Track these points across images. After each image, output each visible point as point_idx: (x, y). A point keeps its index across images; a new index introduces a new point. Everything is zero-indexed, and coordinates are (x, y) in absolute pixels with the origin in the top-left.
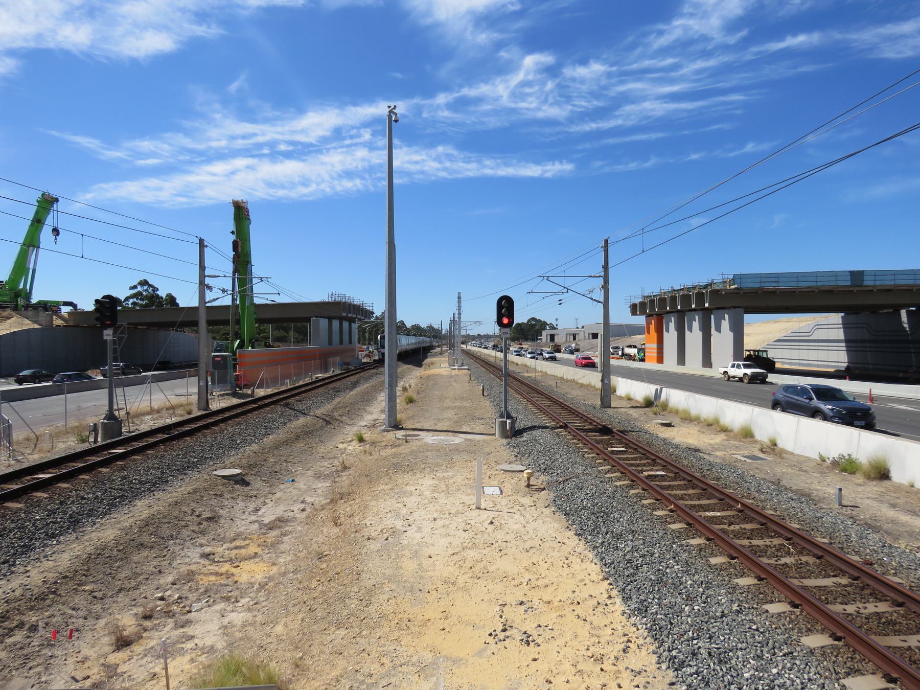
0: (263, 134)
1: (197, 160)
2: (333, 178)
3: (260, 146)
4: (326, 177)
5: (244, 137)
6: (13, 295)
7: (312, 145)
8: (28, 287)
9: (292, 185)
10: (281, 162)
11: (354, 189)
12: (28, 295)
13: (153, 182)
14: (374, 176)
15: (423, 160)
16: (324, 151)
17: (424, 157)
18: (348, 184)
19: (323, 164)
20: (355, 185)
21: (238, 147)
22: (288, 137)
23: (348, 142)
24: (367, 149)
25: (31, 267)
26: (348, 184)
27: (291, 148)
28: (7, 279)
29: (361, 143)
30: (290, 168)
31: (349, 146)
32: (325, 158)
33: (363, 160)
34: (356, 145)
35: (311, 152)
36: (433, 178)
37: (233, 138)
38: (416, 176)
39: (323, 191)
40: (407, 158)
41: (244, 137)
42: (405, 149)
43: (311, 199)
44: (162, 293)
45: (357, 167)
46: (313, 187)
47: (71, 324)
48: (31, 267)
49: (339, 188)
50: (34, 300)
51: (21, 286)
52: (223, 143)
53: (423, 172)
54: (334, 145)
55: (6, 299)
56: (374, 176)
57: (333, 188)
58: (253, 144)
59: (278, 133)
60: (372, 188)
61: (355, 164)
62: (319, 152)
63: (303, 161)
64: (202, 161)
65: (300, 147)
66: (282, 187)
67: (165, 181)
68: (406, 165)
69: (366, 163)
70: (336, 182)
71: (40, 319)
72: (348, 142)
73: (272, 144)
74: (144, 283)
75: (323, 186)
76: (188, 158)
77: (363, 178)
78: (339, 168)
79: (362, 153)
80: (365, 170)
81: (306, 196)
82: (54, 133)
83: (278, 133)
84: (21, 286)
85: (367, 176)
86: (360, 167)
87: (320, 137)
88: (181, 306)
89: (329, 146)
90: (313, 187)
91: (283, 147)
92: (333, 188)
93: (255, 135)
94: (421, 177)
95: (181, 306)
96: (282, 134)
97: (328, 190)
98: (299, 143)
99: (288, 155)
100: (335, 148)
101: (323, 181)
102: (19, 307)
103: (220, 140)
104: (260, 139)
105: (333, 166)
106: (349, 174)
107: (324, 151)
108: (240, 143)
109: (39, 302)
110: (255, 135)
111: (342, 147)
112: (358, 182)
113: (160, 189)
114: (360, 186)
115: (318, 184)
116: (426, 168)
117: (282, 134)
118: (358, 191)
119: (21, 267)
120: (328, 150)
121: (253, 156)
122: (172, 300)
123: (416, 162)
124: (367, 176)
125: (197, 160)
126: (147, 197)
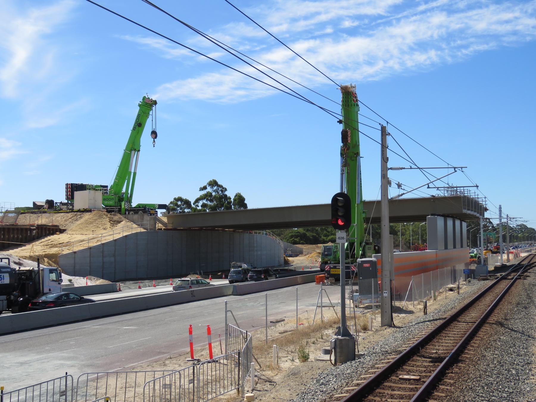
0: (326, 12)
1: (258, 48)
2: (403, 52)
3: (322, 25)
4: (395, 52)
5: (306, 18)
6: (117, 199)
7: (380, 17)
8: (129, 192)
9: (357, 65)
10: (345, 40)
11: (428, 62)
12: (129, 201)
13: (214, 77)
14: (452, 44)
15: (516, 18)
16: (394, 22)
17: (517, 14)
18: (421, 58)
19: (392, 37)
20: (429, 58)
21: (299, 29)
22: (353, 12)
23: (422, 8)
24: (444, 13)
25: (133, 171)
26: (421, 58)
27: (356, 23)
28: (112, 184)
29: (437, 7)
30: (356, 46)
31: (423, 12)
32: (395, 30)
33: (440, 26)
34: (432, 10)
35: (379, 25)
36: (528, 39)
37: (294, 20)
38: (505, 39)
39: (391, 68)
40: (495, 18)
41: (306, 18)
42: (493, 7)
43: (376, 79)
44: (231, 194)
45: (432, 36)
46: (380, 65)
47: (170, 227)
48: (133, 171)
49: (409, 64)
50: (134, 204)
51: (124, 190)
52: (284, 27)
53: (515, 33)
54: (405, 13)
55: (111, 203)
56: (452, 44)
57: (402, 64)
58: (316, 24)
59: (342, 8)
60: (449, 60)
61: (429, 33)
62: (389, 23)
63: (369, 36)
64: (263, 50)
65: (366, 21)
66: (346, 69)
67: (225, 74)
68: (494, 27)
69: (443, 30)
70: (407, 57)
71: (145, 222)
72: (422, 8)
73: (335, 22)
74: (214, 183)
75: (391, 63)
76: (248, 47)
77: (439, 48)
78: (410, 40)
79: (438, 19)
80: (442, 38)
81: (372, 76)
82: (128, 38)
83: (342, 8)
84: (124, 190)
85: (444, 46)
86: (436, 36)
87: (390, 7)
88: (250, 207)
89: (400, 16)
90: (380, 65)
91: (347, 24)
92: (402, 64)
93: (318, 13)
94: (513, 38)
95: (250, 207)
96: (347, 8)
97: (397, 67)
98: (366, 16)
99: (353, 32)
100: (407, 17)
101: (392, 56)
102: (123, 211)
103: (281, 24)
104: (323, 18)
105: (403, 38)
106: (422, 46)
107: (394, 22)
108: (302, 25)
109: (139, 206)
110: (318, 13)
111: (416, 15)
112: (433, 54)
113: (220, 83)
114: (435, 59)
115: (385, 62)
116: (519, 28)
117: (347, 8)
118: (433, 64)
119: (125, 172)
120: (398, 20)
121: (314, 38)
122: (240, 200)
123: (507, 22)
124: (444, 46)
125: (258, 48)
126: (208, 94)
